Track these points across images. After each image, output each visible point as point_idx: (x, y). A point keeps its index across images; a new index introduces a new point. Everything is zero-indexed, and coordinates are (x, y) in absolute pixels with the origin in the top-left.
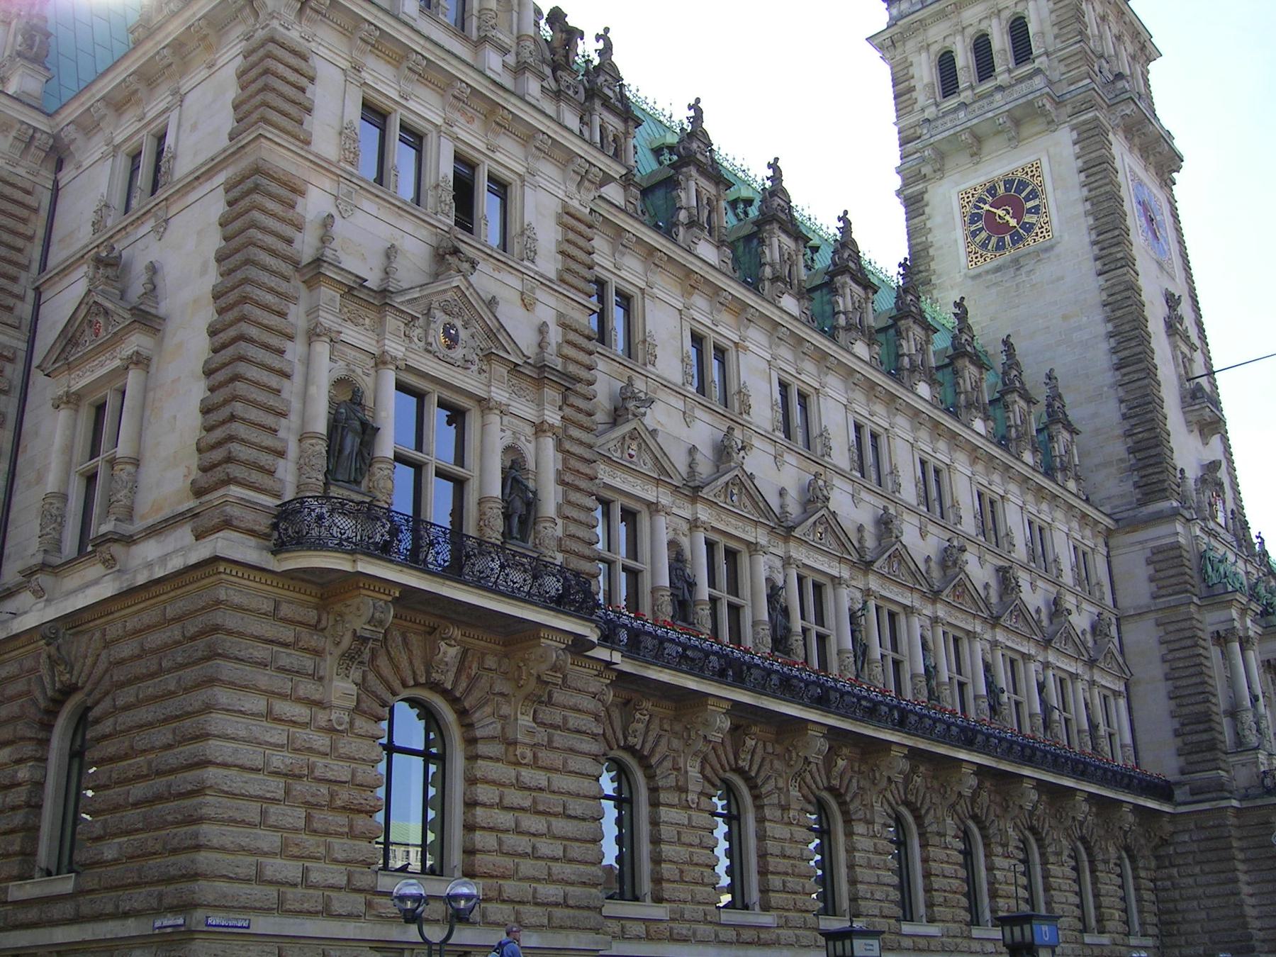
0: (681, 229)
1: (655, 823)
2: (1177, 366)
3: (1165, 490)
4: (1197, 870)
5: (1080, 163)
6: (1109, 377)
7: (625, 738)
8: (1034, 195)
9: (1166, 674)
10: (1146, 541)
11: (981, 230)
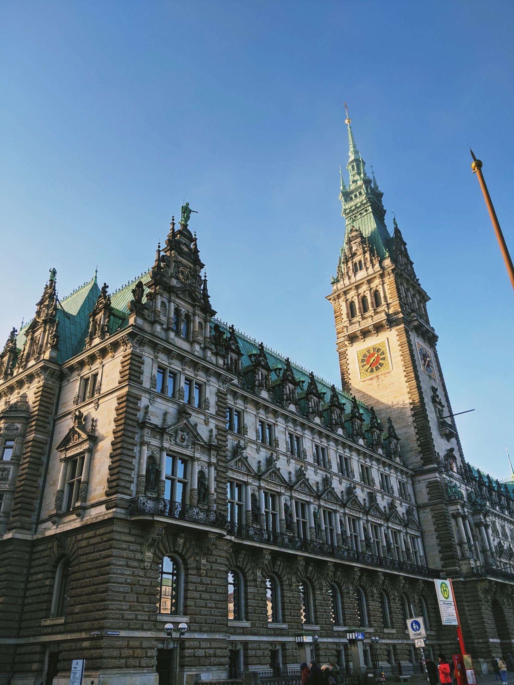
0: (256, 388)
1: (246, 593)
2: (436, 413)
5: (399, 342)
7: (236, 563)
8: (383, 353)
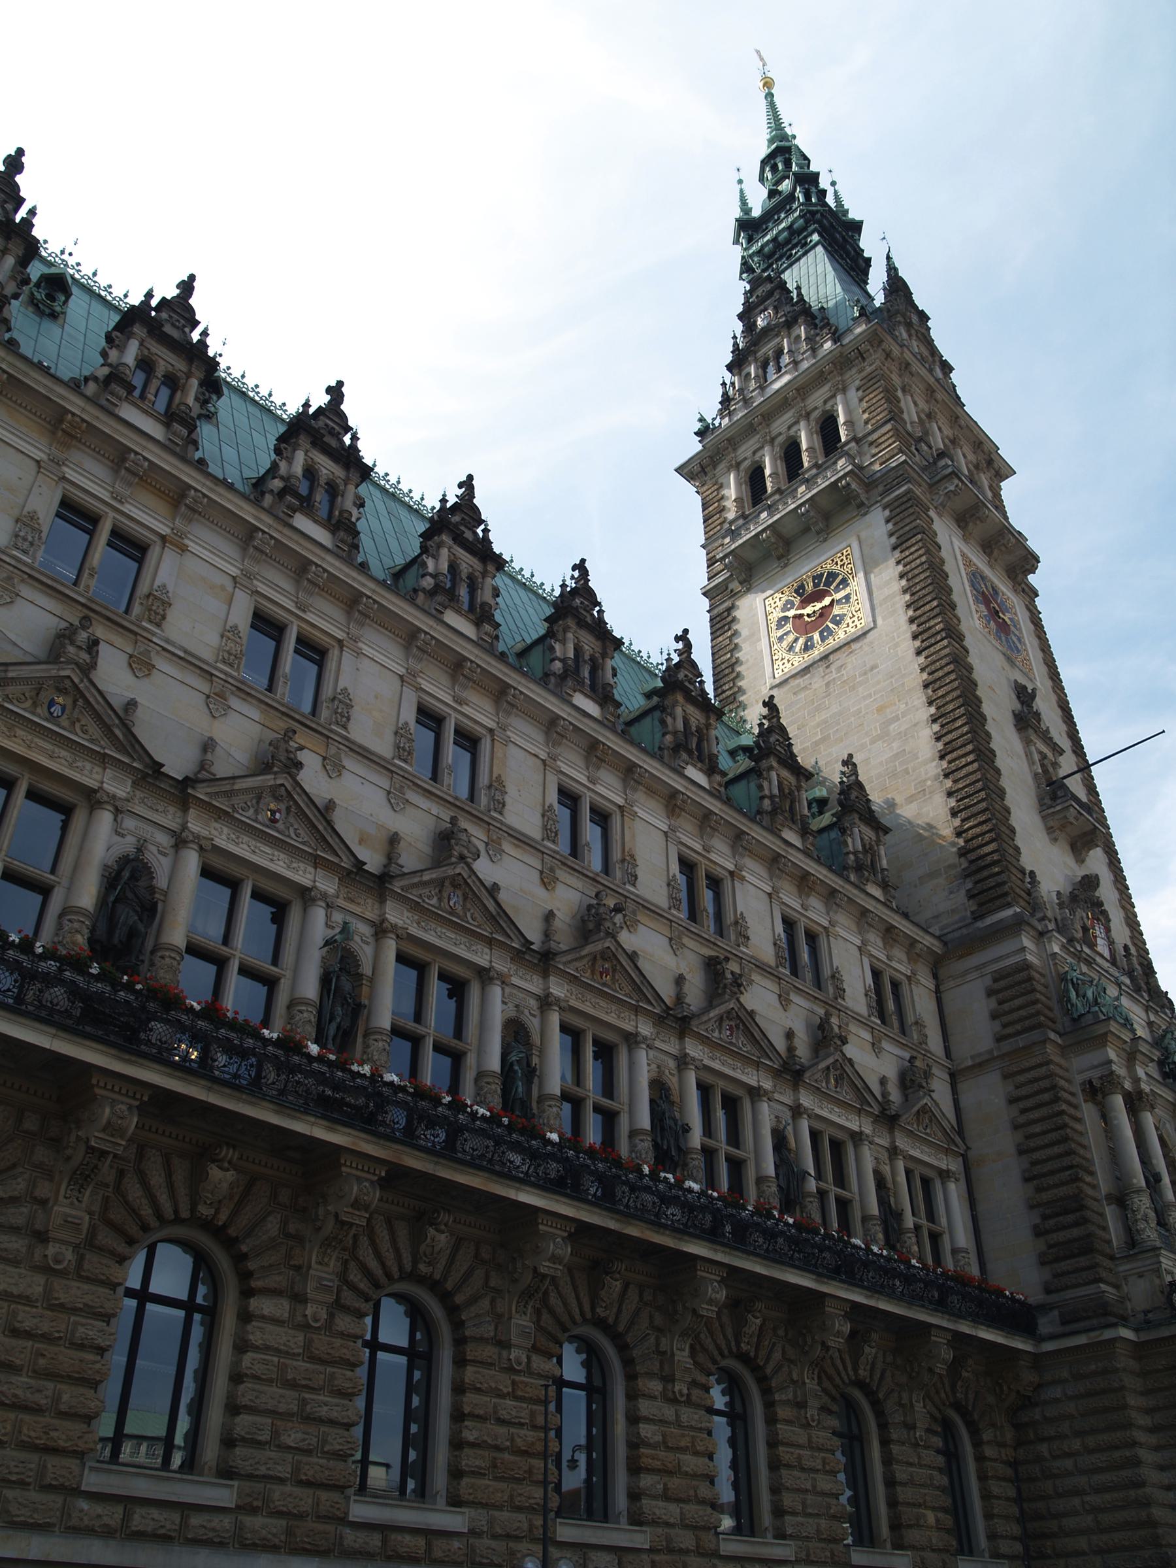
2: (1031, 763)
3: (1006, 894)
4: (1076, 1444)
6: (935, 768)
9: (1019, 1145)
10: (984, 965)
11: (787, 634)
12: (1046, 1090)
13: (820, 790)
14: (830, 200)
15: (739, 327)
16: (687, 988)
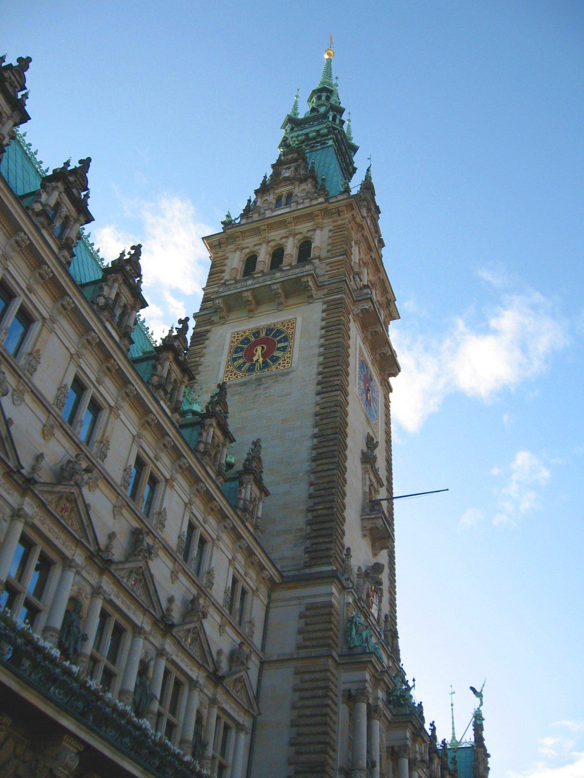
2: (364, 484)
3: (329, 557)
6: (306, 466)
9: (292, 720)
11: (240, 358)
12: (322, 688)
13: (231, 458)
14: (345, 127)
15: (270, 172)
16: (115, 543)
